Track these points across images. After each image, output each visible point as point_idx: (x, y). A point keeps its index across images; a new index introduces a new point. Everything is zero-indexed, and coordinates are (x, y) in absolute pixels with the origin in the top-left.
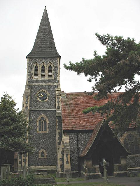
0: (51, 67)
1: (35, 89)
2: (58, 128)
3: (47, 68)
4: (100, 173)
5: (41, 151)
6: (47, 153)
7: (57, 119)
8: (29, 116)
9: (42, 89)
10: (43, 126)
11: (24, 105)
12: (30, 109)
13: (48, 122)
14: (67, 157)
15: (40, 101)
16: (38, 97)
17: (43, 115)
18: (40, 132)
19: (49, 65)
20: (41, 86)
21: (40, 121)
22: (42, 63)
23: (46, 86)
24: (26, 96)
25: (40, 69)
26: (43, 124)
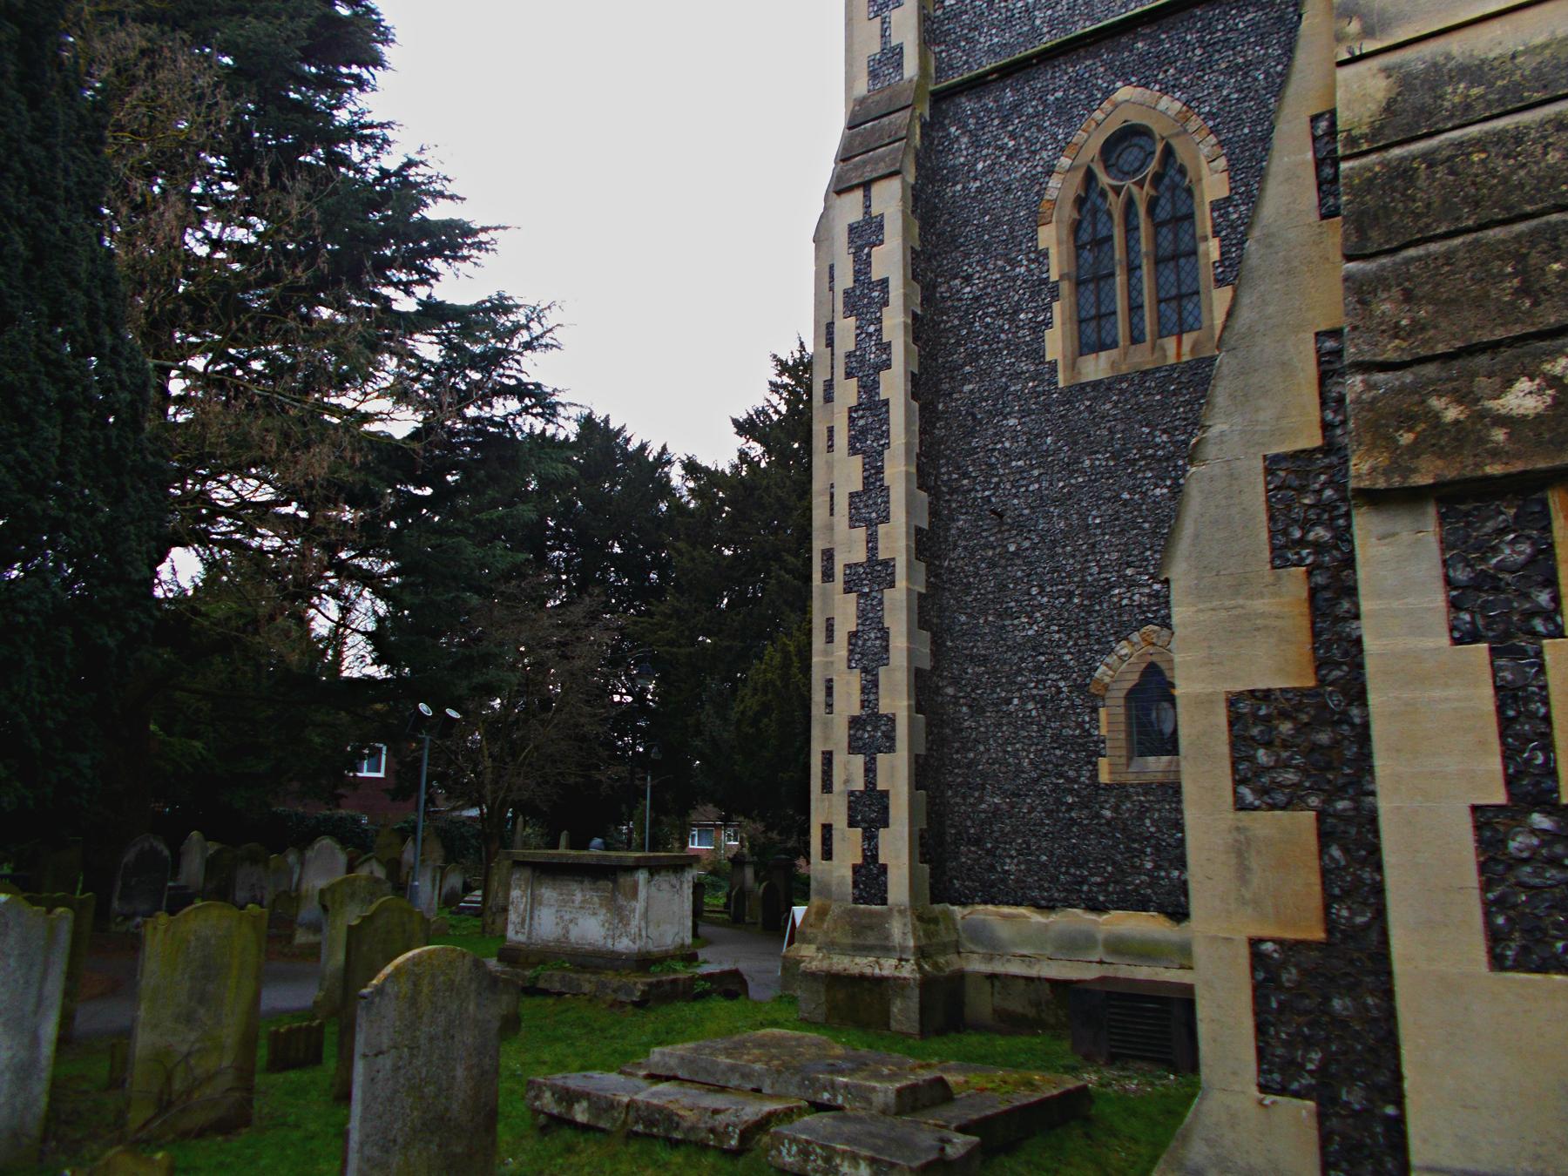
10: (1132, 269)
18: (1096, 368)
21: (1088, 197)
26: (1131, 229)
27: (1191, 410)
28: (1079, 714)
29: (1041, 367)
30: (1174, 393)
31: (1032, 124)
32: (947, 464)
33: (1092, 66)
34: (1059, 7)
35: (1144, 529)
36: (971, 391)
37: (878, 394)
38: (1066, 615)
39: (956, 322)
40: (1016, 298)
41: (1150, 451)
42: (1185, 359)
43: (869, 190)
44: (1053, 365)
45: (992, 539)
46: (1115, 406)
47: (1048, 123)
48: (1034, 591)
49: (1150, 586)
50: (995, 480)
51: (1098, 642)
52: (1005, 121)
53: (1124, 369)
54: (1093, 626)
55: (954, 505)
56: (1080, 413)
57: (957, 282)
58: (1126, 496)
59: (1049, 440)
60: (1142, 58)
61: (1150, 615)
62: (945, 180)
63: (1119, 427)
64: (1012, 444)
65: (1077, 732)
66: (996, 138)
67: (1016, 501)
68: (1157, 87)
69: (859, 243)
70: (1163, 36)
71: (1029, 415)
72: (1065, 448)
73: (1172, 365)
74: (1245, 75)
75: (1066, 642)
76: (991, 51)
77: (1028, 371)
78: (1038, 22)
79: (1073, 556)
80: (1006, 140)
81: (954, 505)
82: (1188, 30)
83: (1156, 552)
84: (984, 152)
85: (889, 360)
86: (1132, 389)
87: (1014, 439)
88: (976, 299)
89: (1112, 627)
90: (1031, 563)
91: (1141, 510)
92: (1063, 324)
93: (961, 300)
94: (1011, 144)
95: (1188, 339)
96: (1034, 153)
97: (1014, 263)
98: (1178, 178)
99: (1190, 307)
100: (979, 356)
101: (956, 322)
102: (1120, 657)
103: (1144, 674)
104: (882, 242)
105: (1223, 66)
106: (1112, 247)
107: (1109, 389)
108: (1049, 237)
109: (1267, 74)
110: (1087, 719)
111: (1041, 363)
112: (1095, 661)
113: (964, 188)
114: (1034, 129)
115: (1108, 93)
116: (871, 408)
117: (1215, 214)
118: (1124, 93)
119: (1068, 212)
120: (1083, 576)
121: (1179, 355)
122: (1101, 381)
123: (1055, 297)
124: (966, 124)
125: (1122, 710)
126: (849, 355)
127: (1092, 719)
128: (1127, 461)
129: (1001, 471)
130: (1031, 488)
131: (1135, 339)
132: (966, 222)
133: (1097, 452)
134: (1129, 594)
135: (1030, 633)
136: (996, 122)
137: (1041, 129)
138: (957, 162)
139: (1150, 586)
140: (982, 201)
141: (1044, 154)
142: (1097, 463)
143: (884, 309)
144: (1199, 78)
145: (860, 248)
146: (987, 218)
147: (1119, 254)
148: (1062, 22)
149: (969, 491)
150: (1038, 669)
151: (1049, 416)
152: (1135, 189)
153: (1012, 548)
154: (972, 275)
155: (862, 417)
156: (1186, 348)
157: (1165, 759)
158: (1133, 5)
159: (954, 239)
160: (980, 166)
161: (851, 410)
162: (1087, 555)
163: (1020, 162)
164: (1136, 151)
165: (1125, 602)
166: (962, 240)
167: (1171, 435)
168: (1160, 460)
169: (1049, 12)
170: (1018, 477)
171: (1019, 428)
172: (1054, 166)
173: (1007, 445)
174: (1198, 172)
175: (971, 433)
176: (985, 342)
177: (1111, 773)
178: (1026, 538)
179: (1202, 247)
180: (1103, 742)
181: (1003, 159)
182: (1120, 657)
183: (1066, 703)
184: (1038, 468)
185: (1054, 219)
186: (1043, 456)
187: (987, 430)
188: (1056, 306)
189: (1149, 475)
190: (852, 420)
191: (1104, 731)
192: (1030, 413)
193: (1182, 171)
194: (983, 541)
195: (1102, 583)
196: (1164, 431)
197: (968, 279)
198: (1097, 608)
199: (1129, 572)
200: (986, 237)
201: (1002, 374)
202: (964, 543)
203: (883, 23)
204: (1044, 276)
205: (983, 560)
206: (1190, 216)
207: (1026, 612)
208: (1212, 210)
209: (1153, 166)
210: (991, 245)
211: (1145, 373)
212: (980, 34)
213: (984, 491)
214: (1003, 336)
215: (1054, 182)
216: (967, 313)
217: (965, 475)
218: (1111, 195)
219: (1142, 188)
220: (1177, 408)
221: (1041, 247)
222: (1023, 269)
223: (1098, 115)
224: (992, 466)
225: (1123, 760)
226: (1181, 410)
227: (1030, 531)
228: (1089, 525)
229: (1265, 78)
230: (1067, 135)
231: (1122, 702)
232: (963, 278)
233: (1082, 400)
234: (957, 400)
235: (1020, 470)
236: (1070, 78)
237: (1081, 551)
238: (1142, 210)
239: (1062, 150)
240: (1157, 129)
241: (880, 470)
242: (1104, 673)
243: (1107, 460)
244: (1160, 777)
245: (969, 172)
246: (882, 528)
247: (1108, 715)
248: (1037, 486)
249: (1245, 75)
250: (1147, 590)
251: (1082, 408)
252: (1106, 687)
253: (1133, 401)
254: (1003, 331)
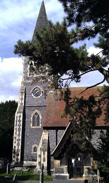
4: (68, 175)
5: (33, 146)
10: (36, 122)
13: (41, 118)
14: (44, 154)
15: (34, 97)
16: (32, 94)
17: (37, 111)
18: (34, 127)
108: (31, 118)
116: (19, 128)
118: (36, 110)
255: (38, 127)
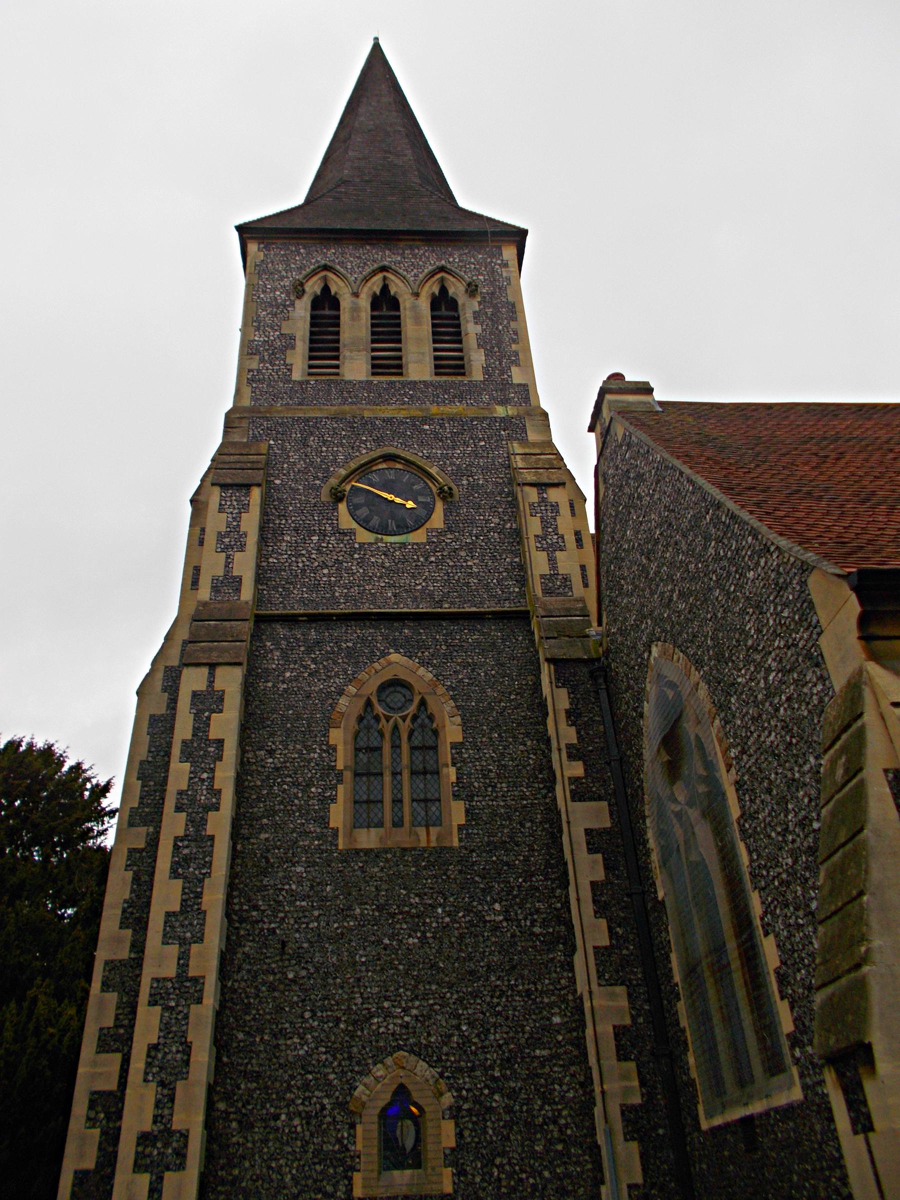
0: (453, 304)
1: (312, 441)
2: (574, 780)
3: (414, 308)
6: (455, 1113)
7: (560, 680)
8: (243, 659)
9: (378, 441)
11: (197, 569)
12: (259, 599)
15: (364, 536)
18: (368, 839)
19: (436, 290)
20: (368, 424)
22: (374, 273)
23: (415, 423)
24: (224, 487)
25: (355, 309)
26: (396, 747)
27: (436, 882)
28: (339, 1130)
29: (325, 830)
30: (425, 868)
31: (330, 658)
32: (239, 896)
33: (376, 634)
34: (352, 590)
35: (399, 970)
36: (267, 839)
37: (205, 830)
38: (333, 1038)
39: (259, 783)
40: (309, 775)
41: (406, 909)
42: (433, 844)
43: (214, 670)
44: (336, 832)
45: (273, 965)
46: (382, 870)
47: (340, 661)
48: (307, 1015)
49: (402, 1018)
50: (281, 915)
51: (359, 1063)
52: (309, 650)
53: (389, 844)
54: (355, 1050)
55: (242, 933)
56: (354, 871)
57: (262, 753)
58: (386, 941)
59: (328, 888)
60: (407, 639)
61: (401, 1043)
62: (260, 677)
63: (385, 886)
64: (297, 887)
65: (337, 1147)
66: (302, 660)
67: (297, 935)
68: (417, 660)
69: (201, 707)
70: (422, 631)
71: (313, 866)
72: (341, 897)
73: (423, 848)
74: (473, 670)
75: (332, 1063)
76: (302, 601)
77: (315, 831)
78: (337, 594)
79: (342, 987)
80: (309, 663)
81: (242, 933)
82: (437, 632)
83: (407, 990)
84: (292, 666)
85: (219, 804)
86: (395, 859)
87: (299, 883)
88: (277, 769)
89: (371, 1051)
90: (306, 990)
91: (397, 954)
92: (345, 802)
93: (264, 767)
94: (313, 666)
95: (434, 831)
96: (330, 677)
97: (311, 750)
98: (427, 721)
99: (434, 809)
100: (275, 813)
101: (259, 783)
102: (376, 1079)
103: (396, 1093)
104: (221, 711)
105: (459, 661)
106: (381, 755)
107: (377, 856)
109: (486, 674)
110: (346, 1135)
111: (326, 827)
112: (355, 1080)
113: (274, 686)
114: (330, 661)
115: (384, 654)
117: (454, 751)
118: (394, 657)
119: (353, 723)
120: (349, 1006)
121: (428, 841)
122: (371, 850)
123: (340, 781)
124: (279, 644)
125: (376, 1126)
126: (180, 793)
127: (349, 1135)
128: (388, 914)
129: (287, 908)
130: (311, 926)
131: (398, 823)
132: (274, 710)
133: (366, 903)
134: (385, 1024)
135: (301, 1052)
136: (302, 649)
137: (335, 663)
138: (270, 667)
139: (402, 1018)
140: (287, 699)
141: (337, 680)
142: (366, 912)
143: (218, 763)
144: (446, 663)
145: (201, 711)
146: (290, 712)
147: (387, 761)
148: (355, 600)
149: (257, 922)
150: (306, 1086)
151: (330, 869)
152: (400, 721)
153: (291, 976)
154: (275, 751)
155: (187, 847)
156: (433, 838)
157: (408, 1172)
158: (402, 606)
159: (263, 720)
160: (288, 674)
161: (176, 839)
162: (353, 987)
163: (319, 680)
164: (399, 696)
165: (381, 1030)
166: (269, 723)
167: (422, 899)
168: (412, 917)
169: (346, 591)
170: (301, 915)
171: (304, 875)
172: (344, 690)
173: (294, 887)
174: (443, 721)
175: (265, 873)
176: (281, 803)
177: (364, 1187)
178: (303, 968)
179: (445, 770)
180: (359, 1157)
181: (306, 675)
182: (376, 1079)
183: (328, 1119)
184: (319, 909)
185: (342, 725)
186: (322, 900)
187: (277, 872)
188: (340, 788)
189: (405, 926)
190: (176, 847)
191: (359, 1146)
192: (315, 864)
193: (431, 718)
194: (265, 967)
195: (364, 1012)
196: (417, 895)
197: (271, 753)
198: (359, 1033)
199: (386, 1004)
200: (289, 725)
201: (293, 831)
202: (248, 967)
203: (228, 557)
204: (333, 764)
205: (264, 983)
206: (435, 748)
207: (299, 1034)
208: (452, 748)
209: (412, 709)
210: (292, 732)
211: (404, 850)
212: (294, 588)
213: (270, 923)
214: (296, 801)
215: (343, 701)
216: (268, 777)
217: (256, 907)
218: (383, 720)
219: (404, 721)
220: (426, 879)
221: (331, 743)
222: (316, 756)
223: (376, 665)
224: (279, 903)
225: (375, 1175)
226: (429, 881)
227: (307, 962)
228: (356, 962)
229: (485, 676)
230: (354, 673)
231: (376, 1119)
232: (267, 751)
233: (356, 862)
234: (253, 844)
235: (303, 910)
236: (358, 636)
237: (349, 984)
238: (405, 737)
239: (350, 681)
240: (417, 686)
241: (199, 895)
242: (363, 1093)
243: (373, 910)
244: (404, 1190)
245: (279, 676)
246: (195, 948)
247: (364, 1130)
248: (316, 924)
249: (473, 670)
250: (399, 1021)
251: (356, 868)
252: (363, 1104)
253: (395, 869)
254: (297, 798)
255: (425, 838)
